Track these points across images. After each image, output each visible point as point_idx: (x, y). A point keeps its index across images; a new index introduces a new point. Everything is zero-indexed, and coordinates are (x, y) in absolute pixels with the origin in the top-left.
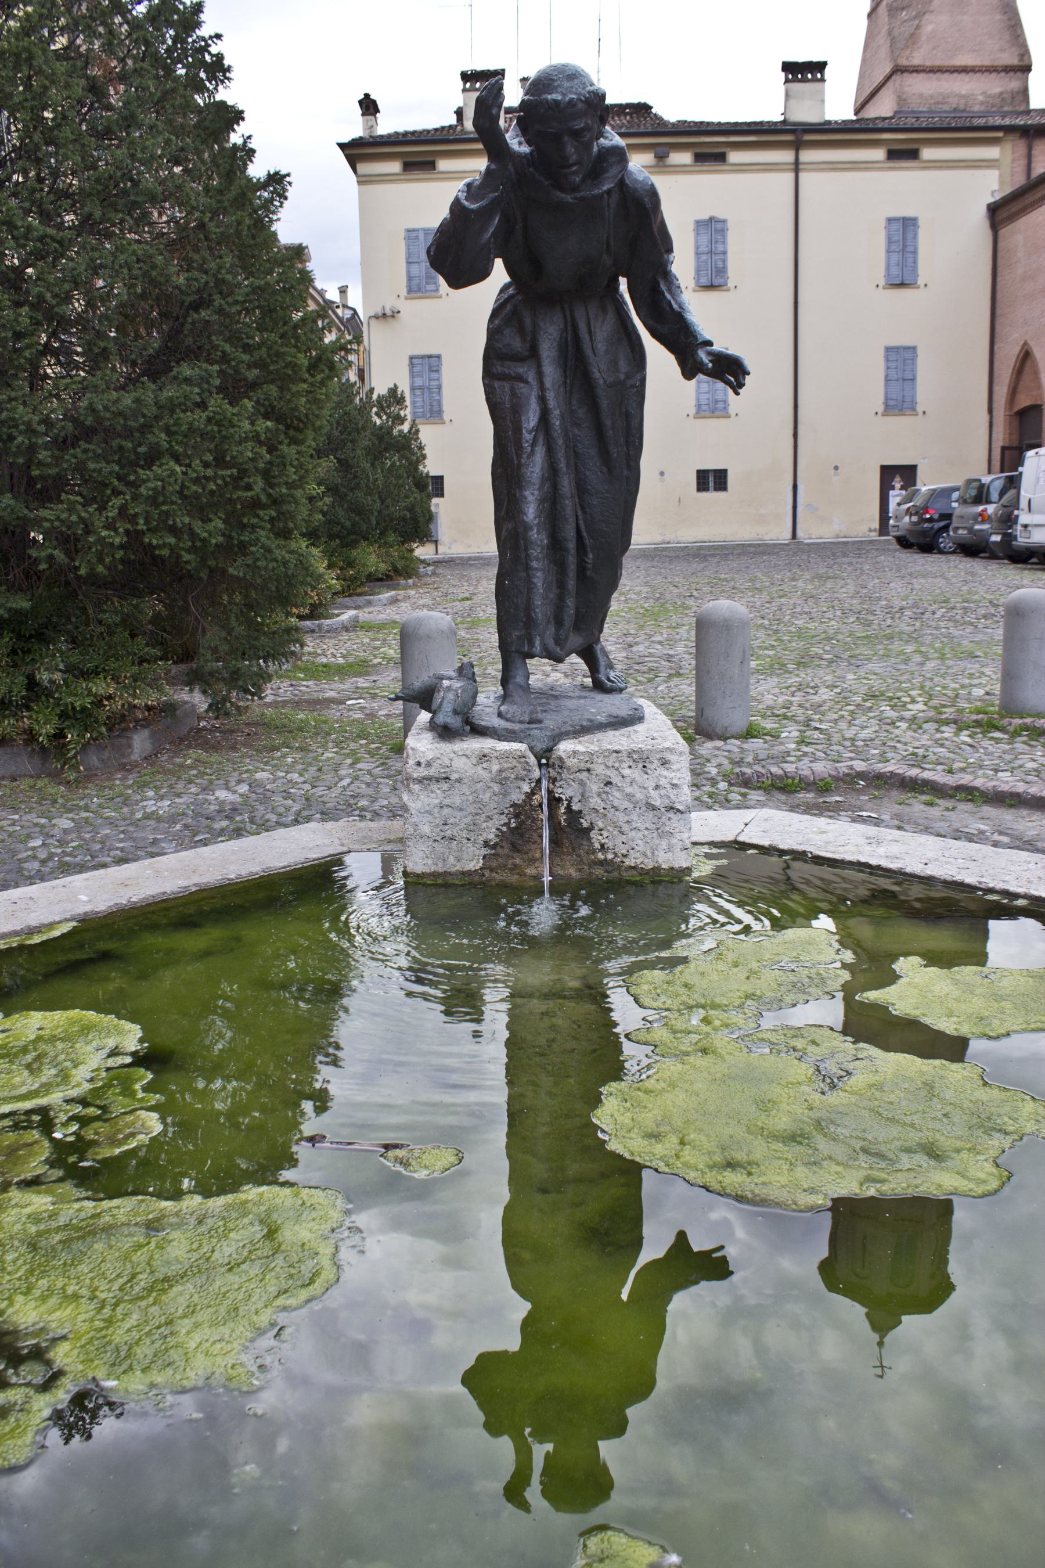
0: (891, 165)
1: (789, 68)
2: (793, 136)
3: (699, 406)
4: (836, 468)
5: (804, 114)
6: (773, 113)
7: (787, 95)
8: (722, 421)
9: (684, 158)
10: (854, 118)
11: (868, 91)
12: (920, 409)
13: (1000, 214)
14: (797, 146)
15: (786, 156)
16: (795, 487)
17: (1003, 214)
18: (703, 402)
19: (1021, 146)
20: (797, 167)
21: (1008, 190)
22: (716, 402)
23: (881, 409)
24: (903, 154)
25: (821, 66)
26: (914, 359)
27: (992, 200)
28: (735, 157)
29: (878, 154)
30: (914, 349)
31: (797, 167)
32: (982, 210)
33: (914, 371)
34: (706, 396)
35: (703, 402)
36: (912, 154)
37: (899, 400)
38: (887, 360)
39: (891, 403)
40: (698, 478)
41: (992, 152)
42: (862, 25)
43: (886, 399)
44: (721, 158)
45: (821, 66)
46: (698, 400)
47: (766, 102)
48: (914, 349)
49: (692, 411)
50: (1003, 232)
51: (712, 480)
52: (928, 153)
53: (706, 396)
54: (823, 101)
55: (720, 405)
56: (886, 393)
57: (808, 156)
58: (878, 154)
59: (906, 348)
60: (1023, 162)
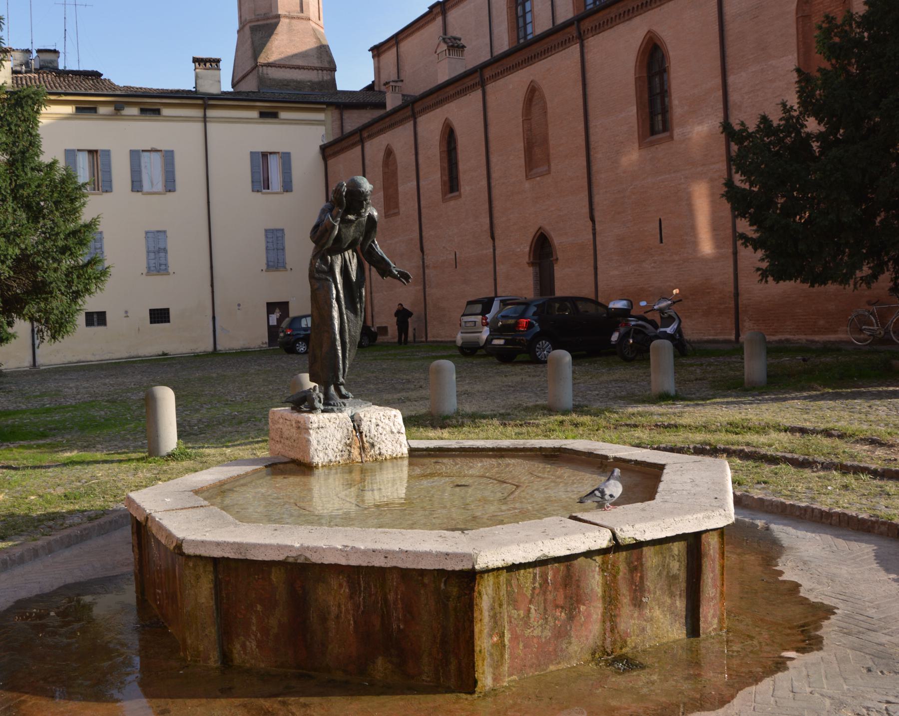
0: (262, 120)
1: (196, 60)
2: (199, 100)
3: (149, 268)
4: (239, 305)
5: (208, 88)
6: (189, 86)
7: (197, 77)
8: (165, 278)
9: (135, 111)
10: (232, 90)
11: (241, 75)
12: (288, 267)
13: (328, 151)
14: (205, 107)
15: (198, 113)
16: (214, 318)
17: (329, 151)
18: (152, 265)
19: (336, 113)
20: (205, 120)
21: (331, 139)
22: (160, 265)
23: (264, 267)
24: (268, 115)
25: (218, 61)
26: (283, 237)
27: (322, 143)
28: (166, 112)
29: (255, 114)
30: (283, 230)
31: (205, 120)
32: (317, 149)
33: (283, 244)
34: (153, 261)
35: (152, 265)
36: (274, 115)
37: (275, 261)
38: (266, 237)
39: (271, 264)
40: (150, 314)
41: (321, 116)
42: (236, 36)
43: (268, 261)
44: (157, 112)
45: (218, 61)
46: (148, 263)
47: (184, 79)
48: (283, 230)
49: (145, 271)
50: (330, 162)
51: (159, 316)
52: (283, 115)
53: (153, 261)
54: (219, 82)
55: (163, 267)
56: (267, 258)
57: (211, 113)
58: (255, 114)
59: (277, 230)
60: (338, 123)
